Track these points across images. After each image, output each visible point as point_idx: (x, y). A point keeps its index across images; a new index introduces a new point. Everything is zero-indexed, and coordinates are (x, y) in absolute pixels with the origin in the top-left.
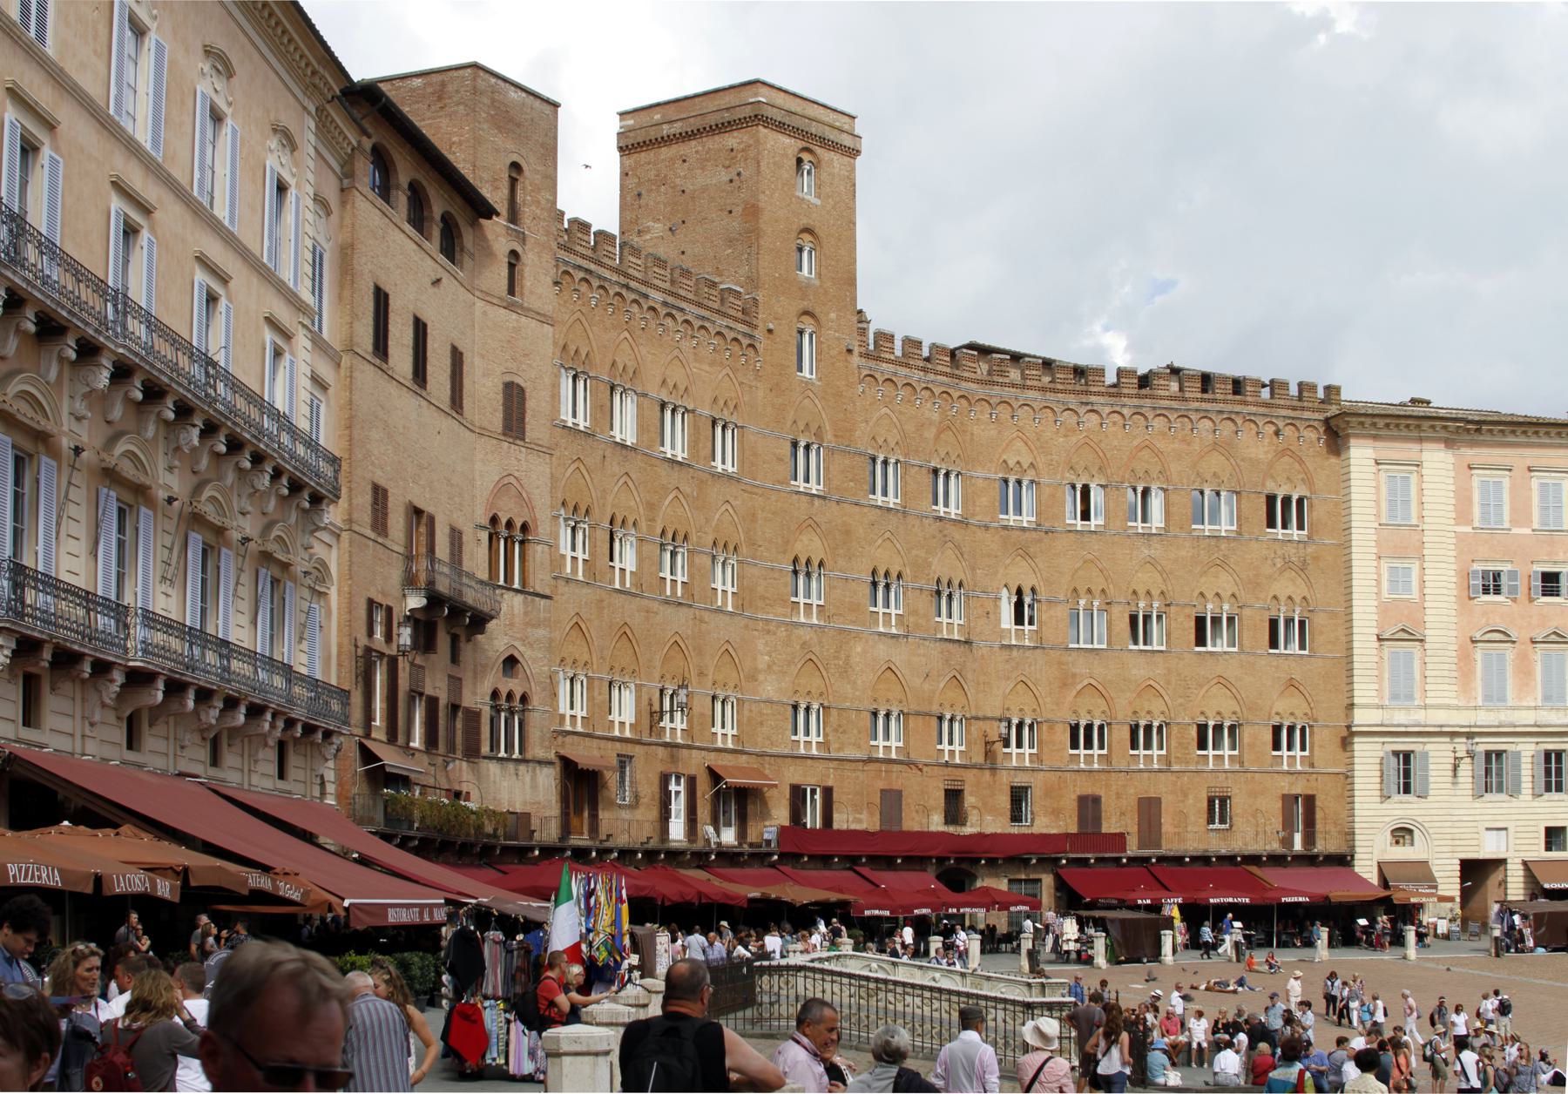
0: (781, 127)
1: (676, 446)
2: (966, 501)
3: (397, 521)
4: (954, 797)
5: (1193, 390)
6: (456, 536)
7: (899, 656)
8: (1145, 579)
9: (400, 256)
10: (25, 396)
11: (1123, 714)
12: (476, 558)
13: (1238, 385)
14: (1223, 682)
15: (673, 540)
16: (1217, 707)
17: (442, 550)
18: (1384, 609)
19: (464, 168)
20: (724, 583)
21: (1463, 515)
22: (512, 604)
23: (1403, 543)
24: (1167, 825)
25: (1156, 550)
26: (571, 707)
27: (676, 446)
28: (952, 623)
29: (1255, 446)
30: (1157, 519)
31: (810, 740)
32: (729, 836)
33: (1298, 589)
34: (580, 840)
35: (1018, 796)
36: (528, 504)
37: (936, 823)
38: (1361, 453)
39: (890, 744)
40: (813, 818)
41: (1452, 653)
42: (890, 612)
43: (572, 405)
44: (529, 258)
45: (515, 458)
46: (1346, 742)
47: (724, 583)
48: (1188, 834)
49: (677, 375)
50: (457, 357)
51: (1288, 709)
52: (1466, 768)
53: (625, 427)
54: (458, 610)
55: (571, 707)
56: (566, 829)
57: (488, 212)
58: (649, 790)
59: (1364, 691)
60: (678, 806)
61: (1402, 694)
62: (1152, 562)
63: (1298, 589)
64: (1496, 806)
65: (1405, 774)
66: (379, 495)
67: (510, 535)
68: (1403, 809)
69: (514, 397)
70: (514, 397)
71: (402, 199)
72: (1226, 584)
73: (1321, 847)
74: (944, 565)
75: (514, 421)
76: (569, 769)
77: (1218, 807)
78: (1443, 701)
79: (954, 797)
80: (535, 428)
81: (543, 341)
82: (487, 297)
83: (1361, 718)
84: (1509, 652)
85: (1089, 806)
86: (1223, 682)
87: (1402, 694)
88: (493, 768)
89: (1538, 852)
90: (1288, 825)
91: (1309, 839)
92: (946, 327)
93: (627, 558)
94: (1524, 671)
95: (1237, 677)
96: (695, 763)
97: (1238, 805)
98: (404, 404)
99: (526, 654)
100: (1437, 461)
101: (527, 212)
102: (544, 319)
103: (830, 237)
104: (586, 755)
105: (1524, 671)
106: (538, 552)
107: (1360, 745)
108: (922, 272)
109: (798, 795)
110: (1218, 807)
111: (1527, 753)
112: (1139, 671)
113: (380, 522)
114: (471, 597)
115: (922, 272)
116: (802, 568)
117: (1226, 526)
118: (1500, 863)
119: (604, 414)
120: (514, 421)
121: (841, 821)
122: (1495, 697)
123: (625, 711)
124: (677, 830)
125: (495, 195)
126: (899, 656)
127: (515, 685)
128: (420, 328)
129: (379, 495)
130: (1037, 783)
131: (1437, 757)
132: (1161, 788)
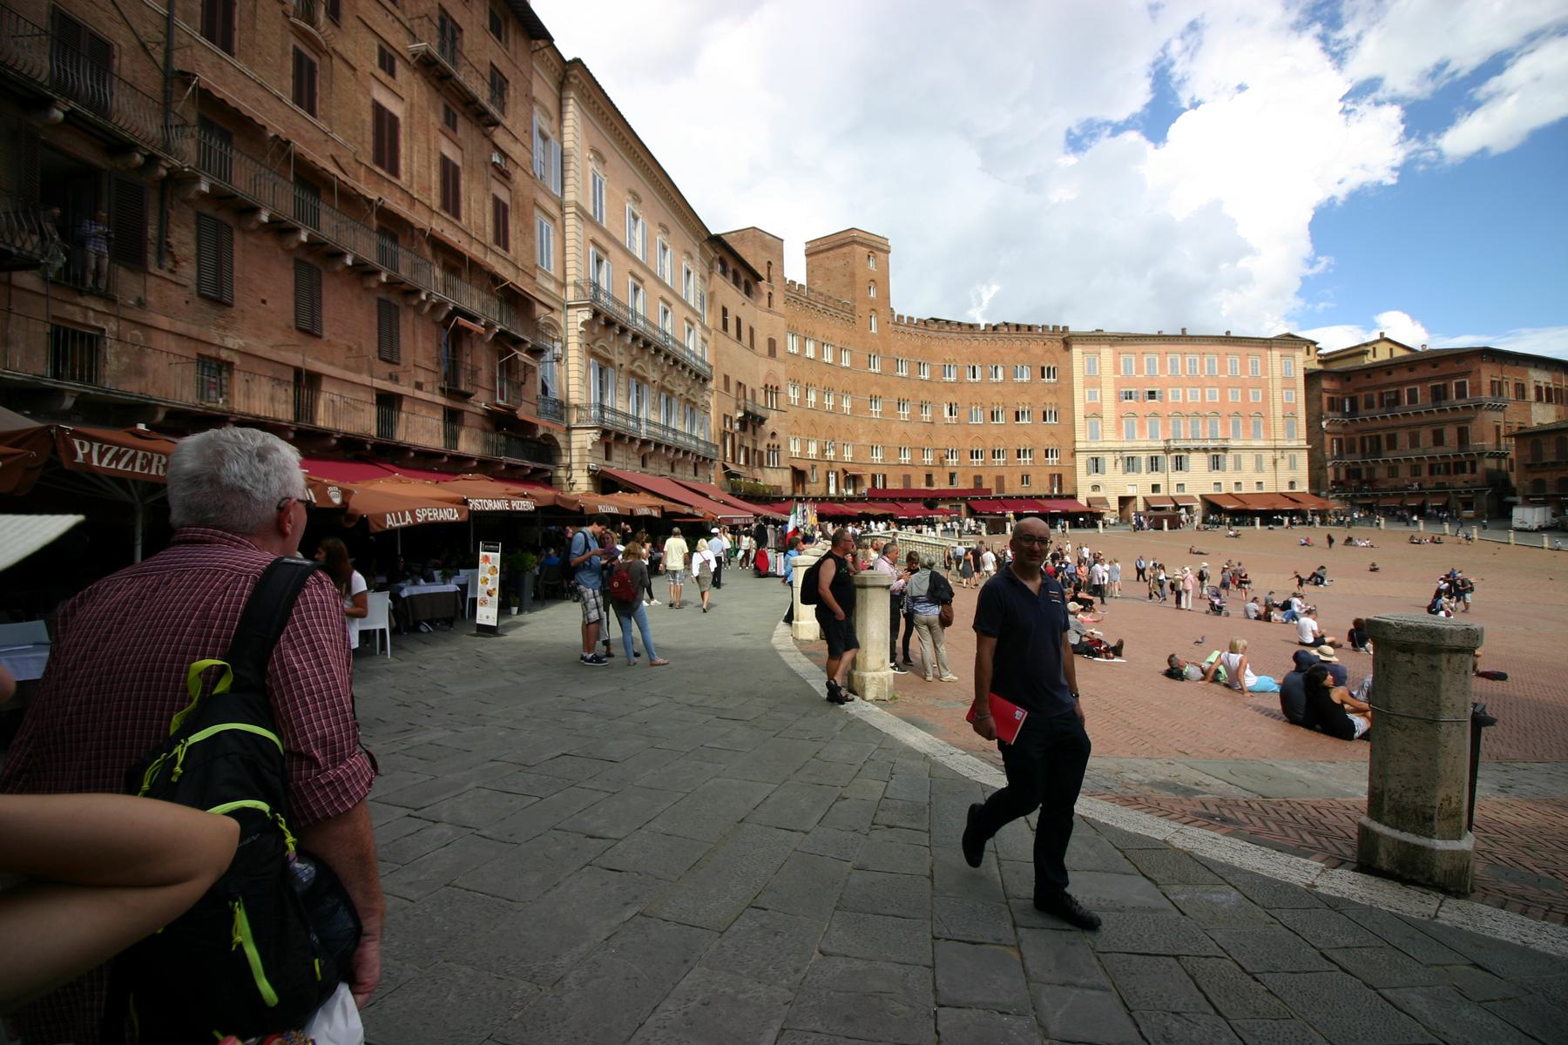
0: (862, 244)
1: (828, 357)
2: (931, 373)
3: (733, 387)
4: (929, 477)
5: (1013, 330)
6: (753, 391)
7: (908, 428)
8: (997, 398)
9: (730, 295)
10: (602, 347)
12: (760, 399)
13: (1030, 328)
14: (1026, 434)
15: (828, 390)
16: (1024, 443)
17: (749, 396)
18: (1087, 407)
19: (751, 263)
20: (846, 405)
21: (1117, 371)
22: (773, 415)
23: (1093, 382)
24: (1007, 485)
25: (1000, 388)
26: (795, 448)
27: (828, 357)
28: (927, 416)
29: (1037, 349)
30: (1000, 378)
31: (878, 458)
32: (850, 492)
33: (1054, 400)
34: (799, 494)
35: (952, 476)
36: (776, 379)
37: (923, 486)
38: (1077, 351)
39: (906, 458)
40: (879, 485)
41: (1113, 422)
42: (905, 413)
43: (793, 345)
44: (776, 295)
45: (774, 364)
46: (1073, 453)
47: (846, 405)
48: (1014, 488)
49: (828, 333)
50: (752, 330)
51: (1050, 443)
52: (1120, 463)
53: (810, 352)
54: (755, 417)
55: (795, 448)
56: (794, 491)
57: (761, 279)
58: (823, 477)
59: (1079, 436)
60: (832, 482)
61: (1094, 436)
62: (998, 392)
63: (1054, 400)
64: (1131, 477)
65: (1096, 465)
66: (727, 378)
67: (772, 390)
68: (1096, 478)
69: (772, 343)
70: (772, 343)
71: (730, 275)
72: (1026, 399)
73: (1066, 492)
74: (924, 396)
75: (772, 352)
76: (794, 469)
77: (1025, 479)
78: (1110, 439)
79: (929, 477)
80: (779, 353)
81: (781, 323)
82: (761, 309)
83: (1079, 446)
84: (1136, 421)
85: (978, 479)
86: (1026, 434)
87: (1094, 436)
88: (768, 471)
89: (1149, 493)
90: (1052, 485)
91: (1060, 489)
92: (921, 312)
93: (812, 397)
94: (1142, 427)
95: (1030, 431)
97: (1032, 478)
98: (734, 347)
99: (778, 431)
100: (1107, 352)
101: (774, 279)
102: (781, 316)
103: (881, 282)
104: (800, 465)
105: (1142, 427)
106: (781, 396)
107: (1078, 456)
108: (914, 293)
109: (874, 477)
110: (1025, 479)
111: (1144, 456)
112: (995, 431)
113: (727, 388)
114: (760, 412)
115: (914, 293)
116: (873, 399)
117: (1026, 379)
118: (1134, 498)
119: (803, 347)
120: (772, 352)
121: (889, 486)
122: (1130, 437)
123: (813, 450)
125: (762, 273)
126: (908, 428)
127: (775, 442)
128: (738, 320)
129: (727, 378)
130: (959, 472)
131: (1109, 459)
132: (1004, 472)
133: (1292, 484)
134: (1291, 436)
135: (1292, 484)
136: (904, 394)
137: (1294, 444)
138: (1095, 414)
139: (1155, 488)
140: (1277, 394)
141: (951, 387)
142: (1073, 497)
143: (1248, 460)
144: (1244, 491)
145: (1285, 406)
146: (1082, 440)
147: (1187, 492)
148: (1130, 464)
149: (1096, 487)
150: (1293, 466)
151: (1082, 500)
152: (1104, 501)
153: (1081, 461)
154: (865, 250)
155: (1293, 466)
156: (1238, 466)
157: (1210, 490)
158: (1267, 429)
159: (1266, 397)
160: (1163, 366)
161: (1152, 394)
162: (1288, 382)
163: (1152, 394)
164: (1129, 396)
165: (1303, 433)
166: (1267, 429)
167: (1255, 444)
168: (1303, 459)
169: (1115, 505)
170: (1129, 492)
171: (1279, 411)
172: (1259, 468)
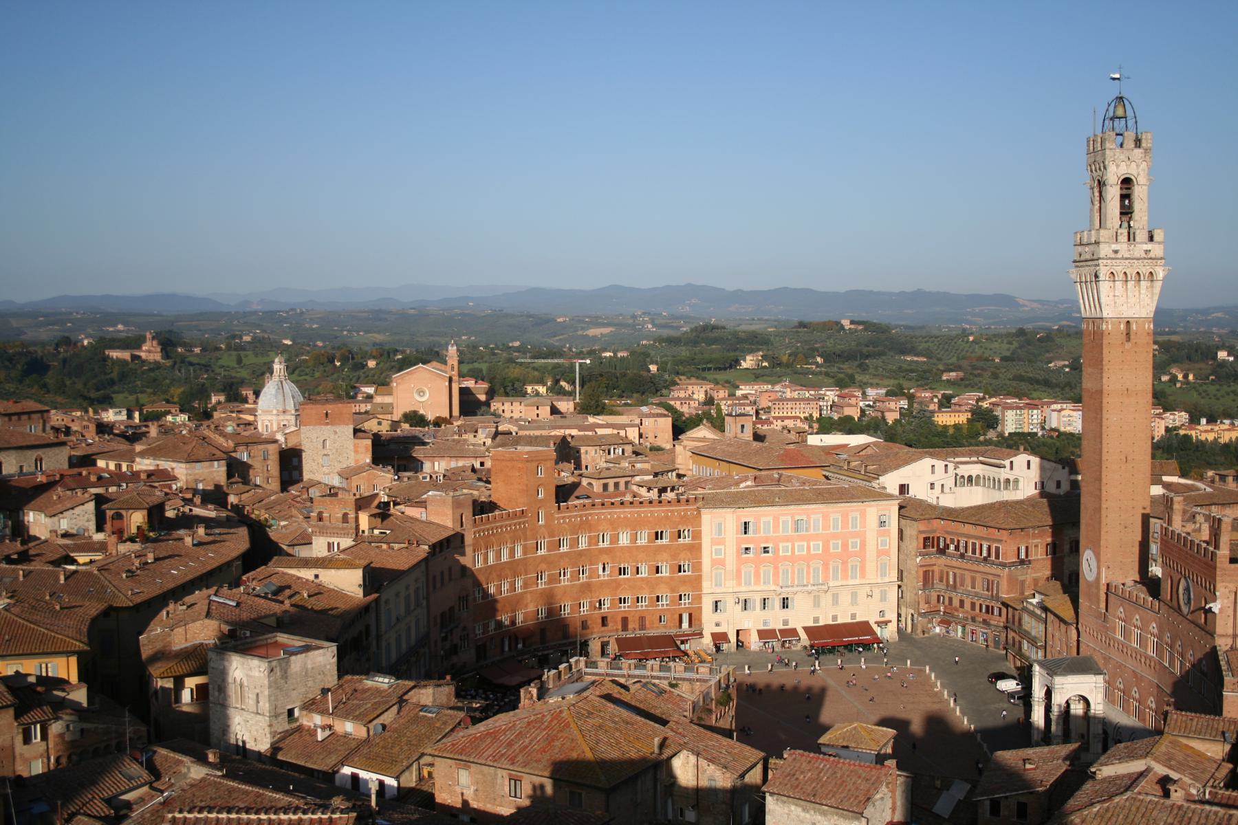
46: (699, 598)
68: (717, 617)
72: (665, 555)
106: (471, 598)
134: (883, 575)
137: (887, 580)
141: (603, 551)
143: (845, 598)
144: (840, 621)
146: (706, 586)
147: (790, 626)
150: (883, 598)
155: (883, 598)
156: (835, 600)
158: (863, 569)
161: (766, 550)
167: (851, 582)
169: (733, 639)
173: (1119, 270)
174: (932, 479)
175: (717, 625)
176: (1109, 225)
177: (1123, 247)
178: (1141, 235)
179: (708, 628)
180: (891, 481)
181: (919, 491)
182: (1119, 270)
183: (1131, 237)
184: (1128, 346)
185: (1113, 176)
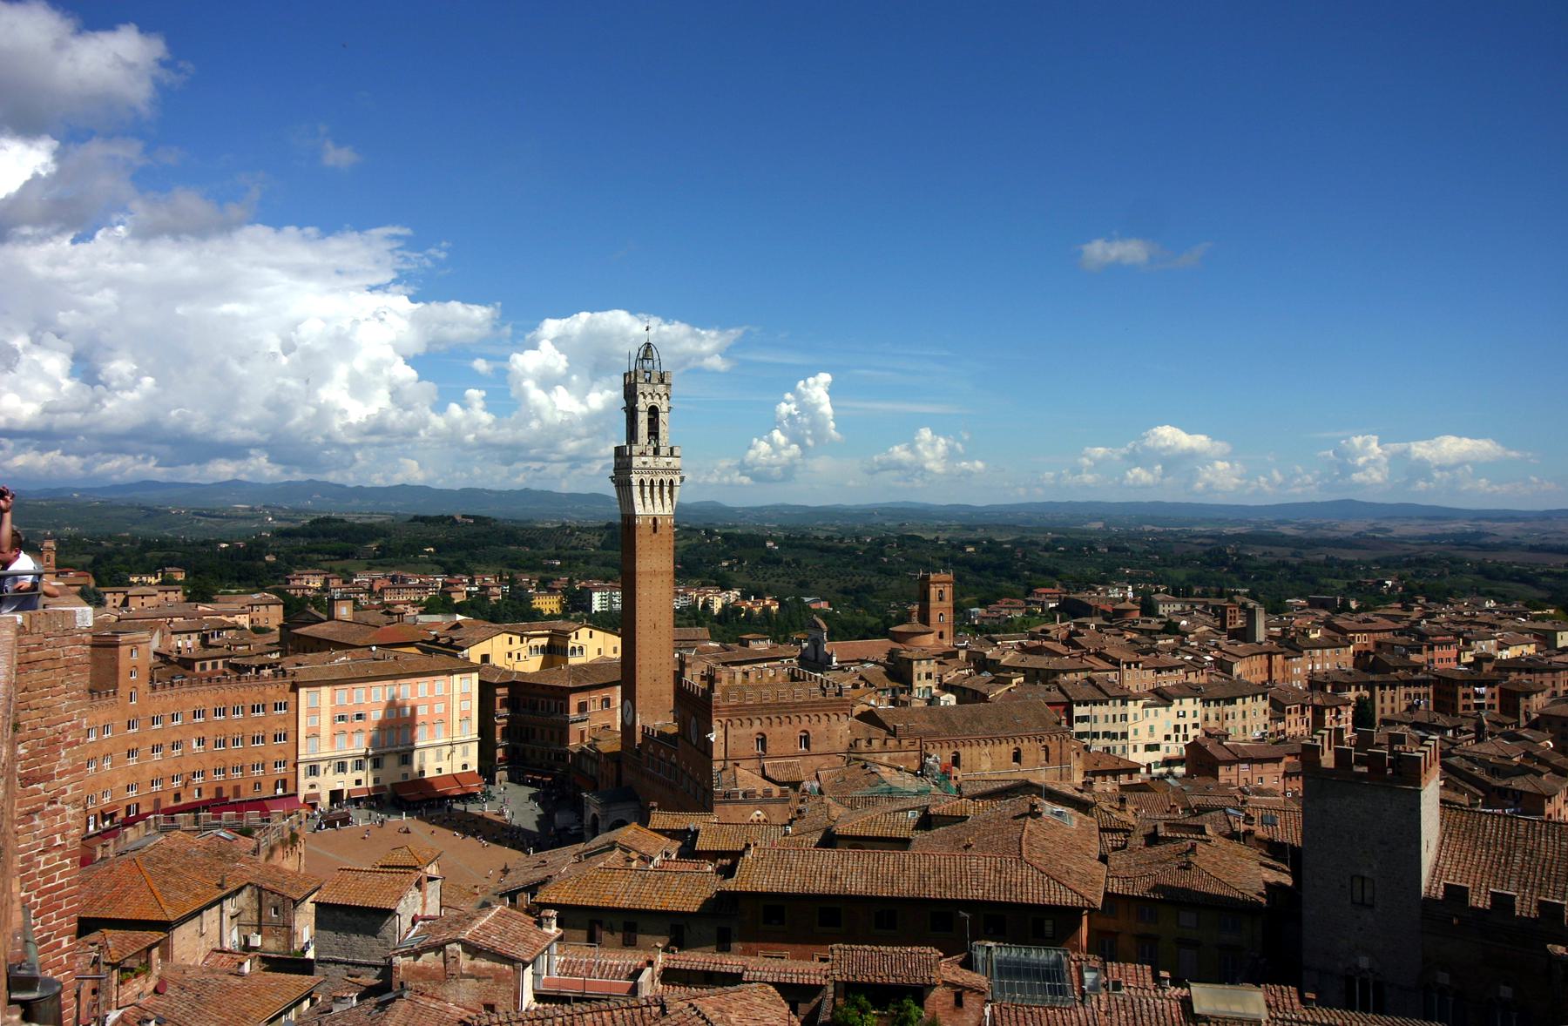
7: (161, 765)
11: (230, 764)
23: (314, 711)
35: (200, 790)
64: (341, 775)
65: (314, 770)
68: (313, 779)
72: (261, 728)
74: (176, 737)
78: (326, 751)
85: (219, 790)
96: (98, 811)
109: (128, 808)
124: (91, 828)
131: (323, 765)
132: (241, 783)
133: (465, 766)
135: (465, 766)
136: (156, 741)
138: (314, 735)
139: (358, 782)
140: (456, 706)
142: (296, 795)
145: (462, 713)
148: (342, 767)
149: (312, 786)
150: (465, 753)
151: (301, 798)
152: (317, 796)
153: (301, 767)
154: (128, 648)
155: (465, 753)
157: (400, 780)
159: (447, 709)
160: (368, 696)
161: (359, 716)
162: (466, 696)
163: (359, 716)
164: (342, 718)
165: (476, 730)
166: (447, 730)
168: (474, 749)
169: (326, 799)
170: (339, 786)
171: (457, 717)
172: (439, 759)
173: (647, 478)
174: (509, 648)
175: (312, 786)
176: (640, 441)
177: (650, 460)
178: (663, 451)
179: (304, 791)
180: (474, 654)
181: (498, 660)
182: (647, 478)
183: (656, 452)
184: (655, 536)
185: (642, 405)
